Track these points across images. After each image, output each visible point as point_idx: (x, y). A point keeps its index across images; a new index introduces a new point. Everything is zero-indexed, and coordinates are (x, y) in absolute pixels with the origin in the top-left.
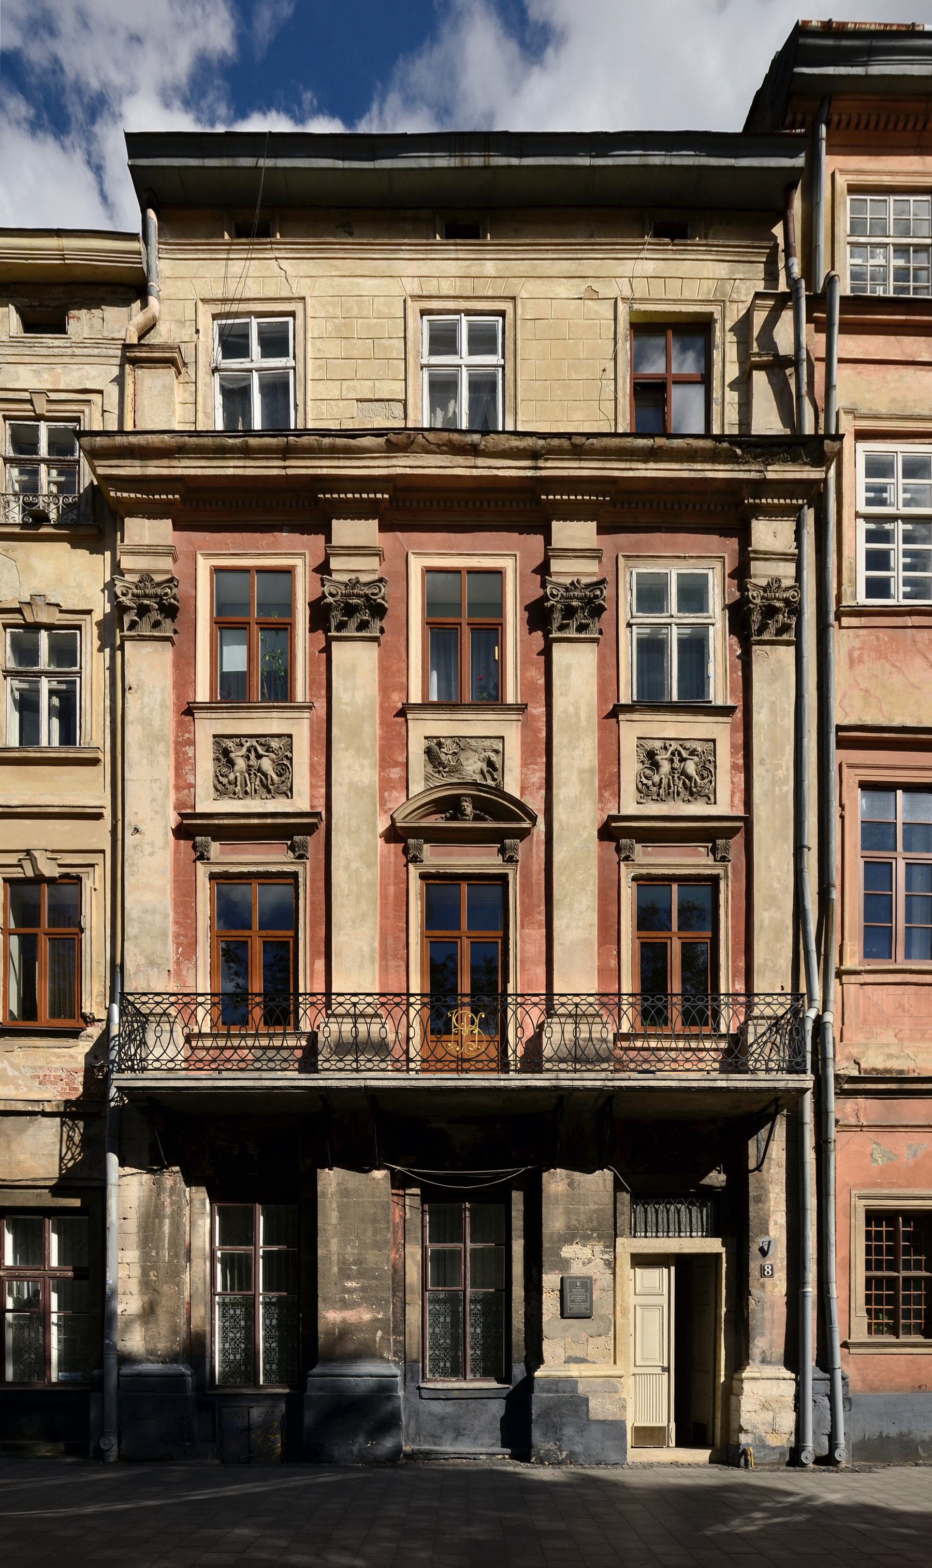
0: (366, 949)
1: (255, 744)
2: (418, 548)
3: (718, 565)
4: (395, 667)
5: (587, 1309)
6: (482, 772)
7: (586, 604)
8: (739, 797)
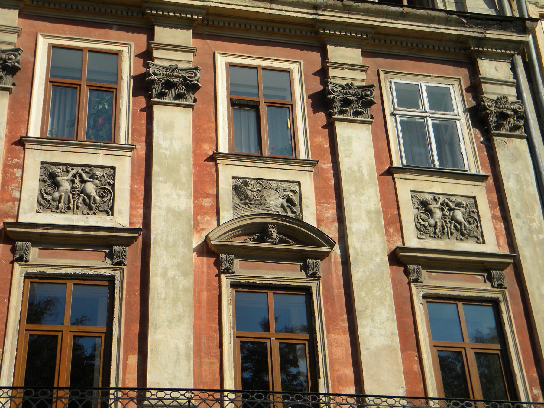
0: (182, 347)
1: (80, 171)
2: (223, 50)
3: (456, 84)
4: (206, 126)
6: (283, 206)
7: (360, 99)
8: (503, 240)
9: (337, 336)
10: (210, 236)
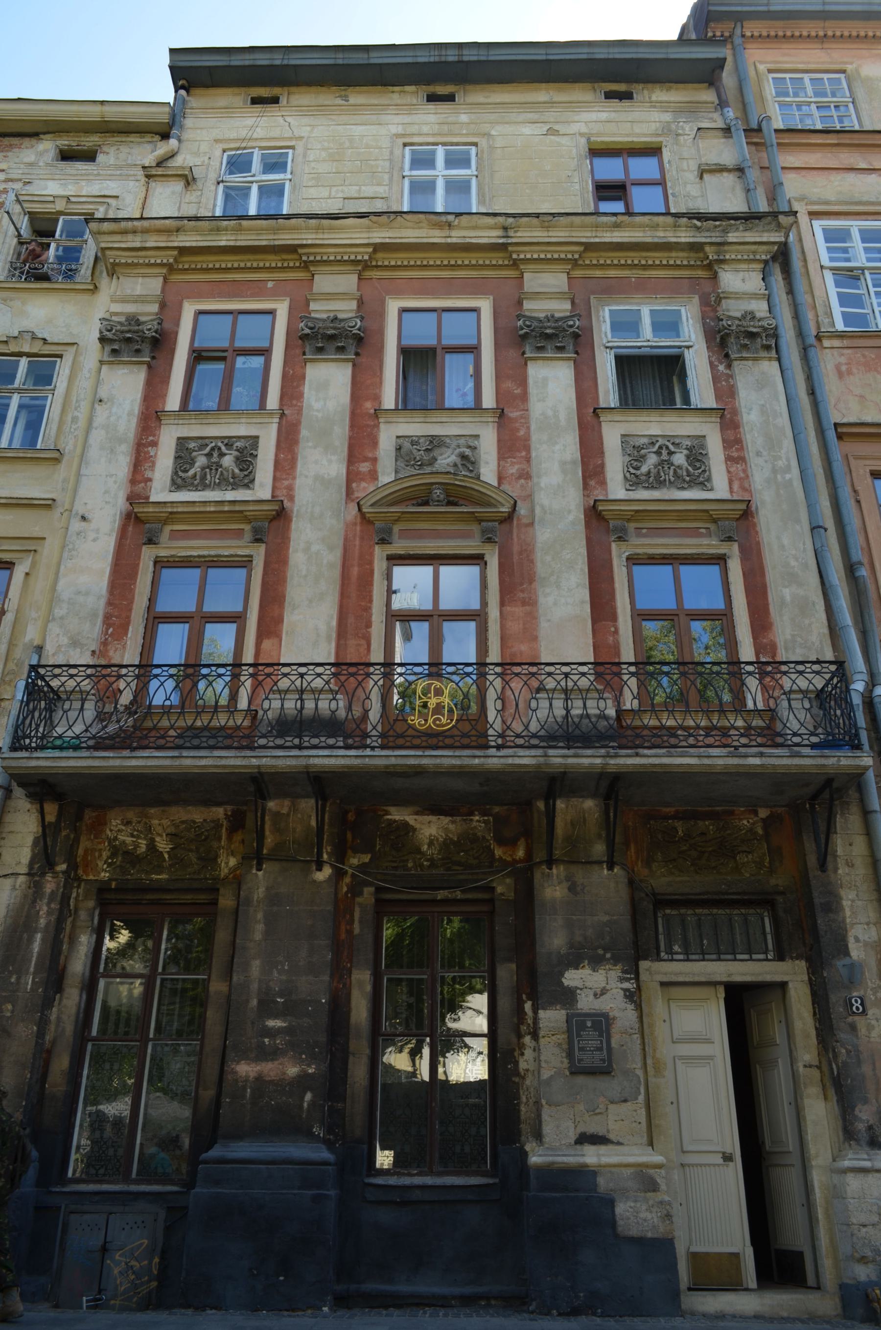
0: (323, 627)
1: (220, 444)
5: (603, 1060)
9: (513, 609)
10: (361, 503)
